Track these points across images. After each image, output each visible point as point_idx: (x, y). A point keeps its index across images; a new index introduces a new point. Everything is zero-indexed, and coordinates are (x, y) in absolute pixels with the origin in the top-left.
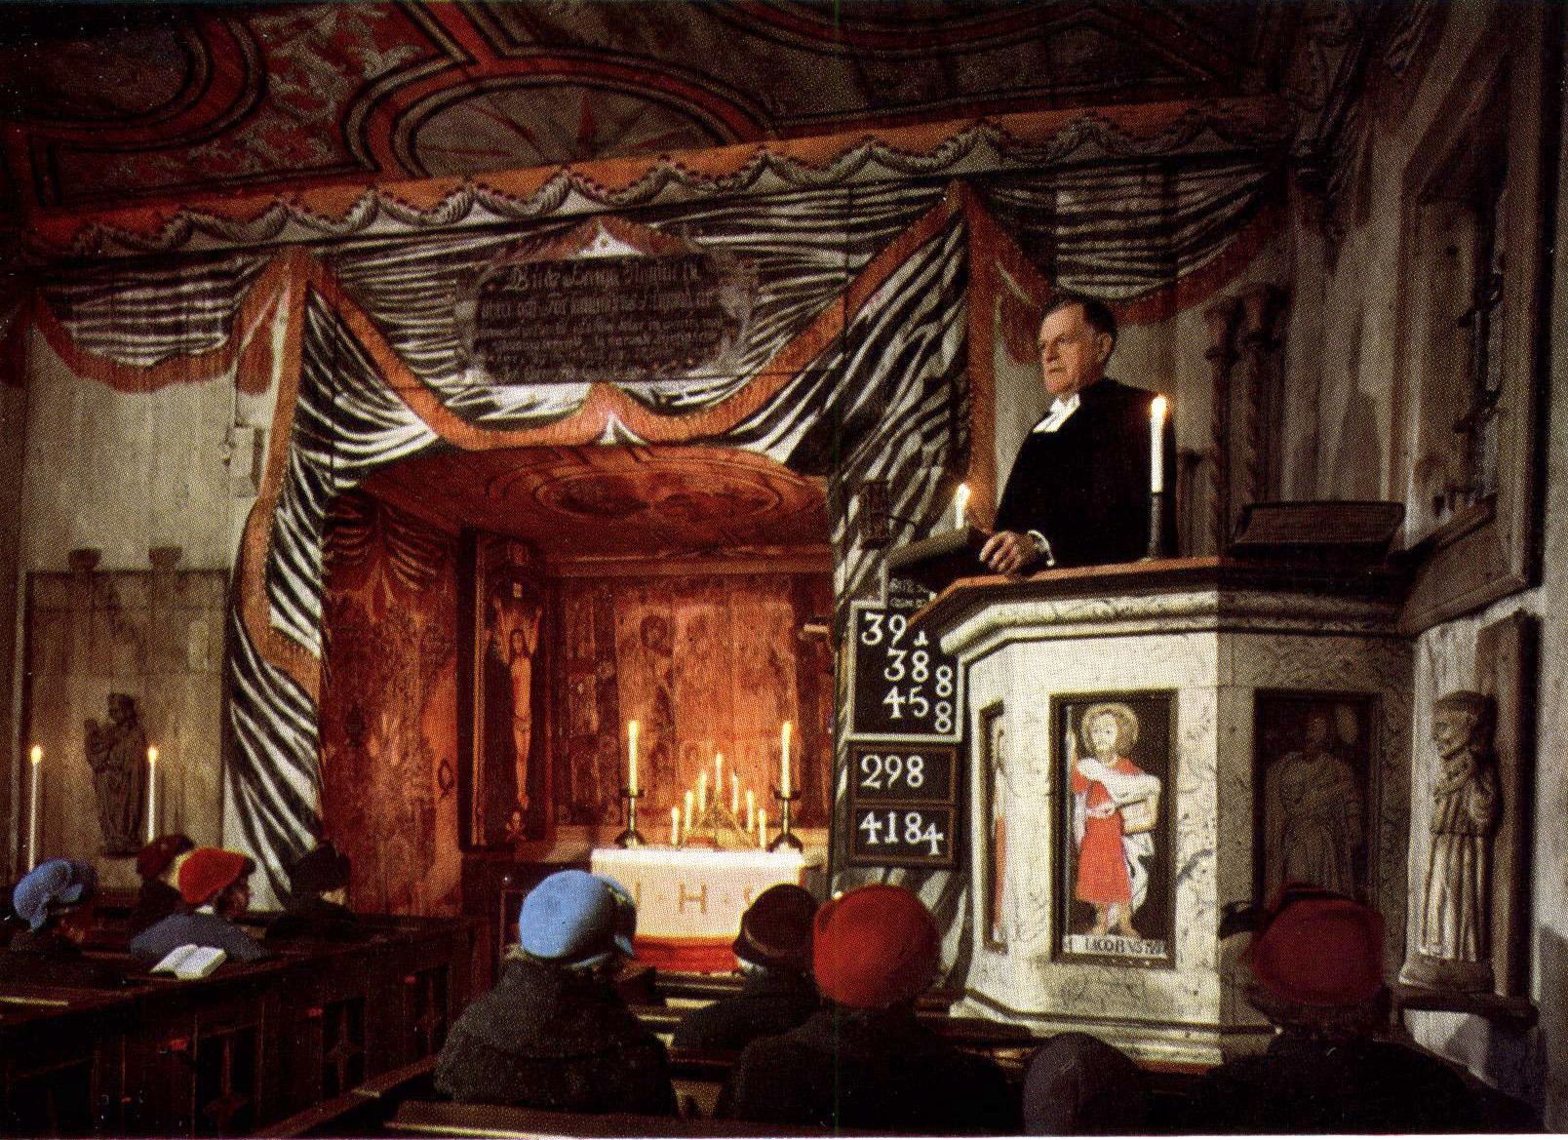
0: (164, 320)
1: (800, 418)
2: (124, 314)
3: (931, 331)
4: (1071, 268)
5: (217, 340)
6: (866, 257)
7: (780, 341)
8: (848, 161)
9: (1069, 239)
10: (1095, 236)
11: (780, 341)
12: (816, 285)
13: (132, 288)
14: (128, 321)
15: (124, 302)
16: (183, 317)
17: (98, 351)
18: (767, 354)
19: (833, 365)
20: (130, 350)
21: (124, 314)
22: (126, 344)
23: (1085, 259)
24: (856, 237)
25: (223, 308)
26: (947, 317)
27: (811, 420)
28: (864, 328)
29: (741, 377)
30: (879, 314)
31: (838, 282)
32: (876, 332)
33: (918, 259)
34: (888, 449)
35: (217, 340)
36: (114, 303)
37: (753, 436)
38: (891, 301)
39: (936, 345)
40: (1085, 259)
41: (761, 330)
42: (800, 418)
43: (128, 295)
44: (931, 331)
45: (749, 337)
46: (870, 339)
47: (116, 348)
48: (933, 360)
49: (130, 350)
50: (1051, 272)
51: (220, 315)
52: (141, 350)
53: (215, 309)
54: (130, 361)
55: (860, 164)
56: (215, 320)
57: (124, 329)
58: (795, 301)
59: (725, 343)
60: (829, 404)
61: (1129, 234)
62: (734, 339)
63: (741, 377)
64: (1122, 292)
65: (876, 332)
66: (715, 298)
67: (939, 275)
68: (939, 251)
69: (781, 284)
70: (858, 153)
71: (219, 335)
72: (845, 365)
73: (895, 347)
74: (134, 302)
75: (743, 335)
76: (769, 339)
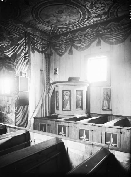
1: (12, 52)
3: (25, 47)
4: (36, 46)
6: (19, 36)
7: (10, 42)
8: (19, 25)
9: (37, 43)
10: (38, 43)
11: (10, 42)
12: (14, 37)
18: (9, 43)
19: (16, 47)
23: (38, 45)
24: (18, 33)
26: (26, 46)
27: (13, 53)
28: (19, 44)
29: (6, 45)
30: (20, 43)
31: (16, 38)
32: (20, 45)
33: (24, 39)
34: (22, 59)
37: (7, 53)
38: (22, 42)
39: (26, 49)
40: (38, 45)
41: (8, 40)
42: (12, 52)
44: (25, 47)
45: (6, 40)
46: (19, 46)
48: (25, 51)
50: (35, 45)
55: (20, 26)
58: (11, 38)
59: (4, 40)
60: (15, 52)
61: (40, 44)
62: (5, 40)
63: (6, 45)
64: (40, 49)
65: (20, 45)
66: (2, 33)
67: (25, 41)
68: (25, 39)
69: (11, 35)
70: (20, 25)
72: (17, 48)
73: (22, 48)
75: (6, 40)
76: (9, 41)
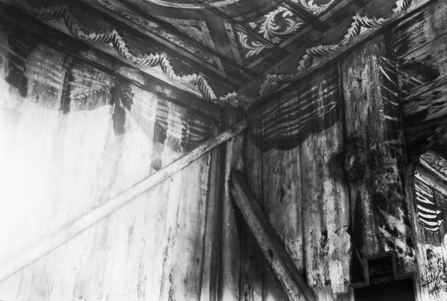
0: (304, 108)
2: (285, 114)
5: (332, 105)
13: (287, 101)
14: (287, 116)
15: (284, 108)
16: (313, 102)
17: (273, 136)
20: (288, 129)
21: (285, 114)
22: (287, 127)
25: (333, 89)
35: (332, 105)
36: (280, 110)
43: (286, 104)
47: (282, 131)
49: (288, 129)
51: (332, 93)
52: (293, 127)
53: (329, 91)
54: (289, 134)
56: (330, 96)
57: (285, 121)
71: (332, 103)
74: (289, 106)
